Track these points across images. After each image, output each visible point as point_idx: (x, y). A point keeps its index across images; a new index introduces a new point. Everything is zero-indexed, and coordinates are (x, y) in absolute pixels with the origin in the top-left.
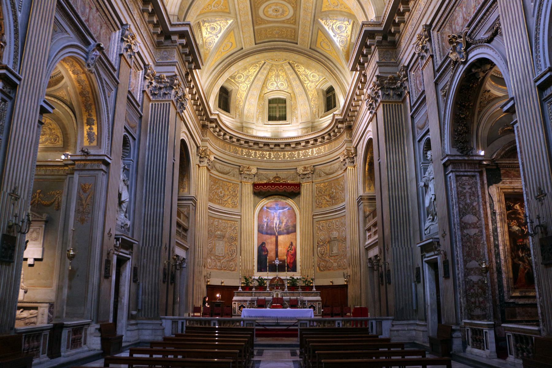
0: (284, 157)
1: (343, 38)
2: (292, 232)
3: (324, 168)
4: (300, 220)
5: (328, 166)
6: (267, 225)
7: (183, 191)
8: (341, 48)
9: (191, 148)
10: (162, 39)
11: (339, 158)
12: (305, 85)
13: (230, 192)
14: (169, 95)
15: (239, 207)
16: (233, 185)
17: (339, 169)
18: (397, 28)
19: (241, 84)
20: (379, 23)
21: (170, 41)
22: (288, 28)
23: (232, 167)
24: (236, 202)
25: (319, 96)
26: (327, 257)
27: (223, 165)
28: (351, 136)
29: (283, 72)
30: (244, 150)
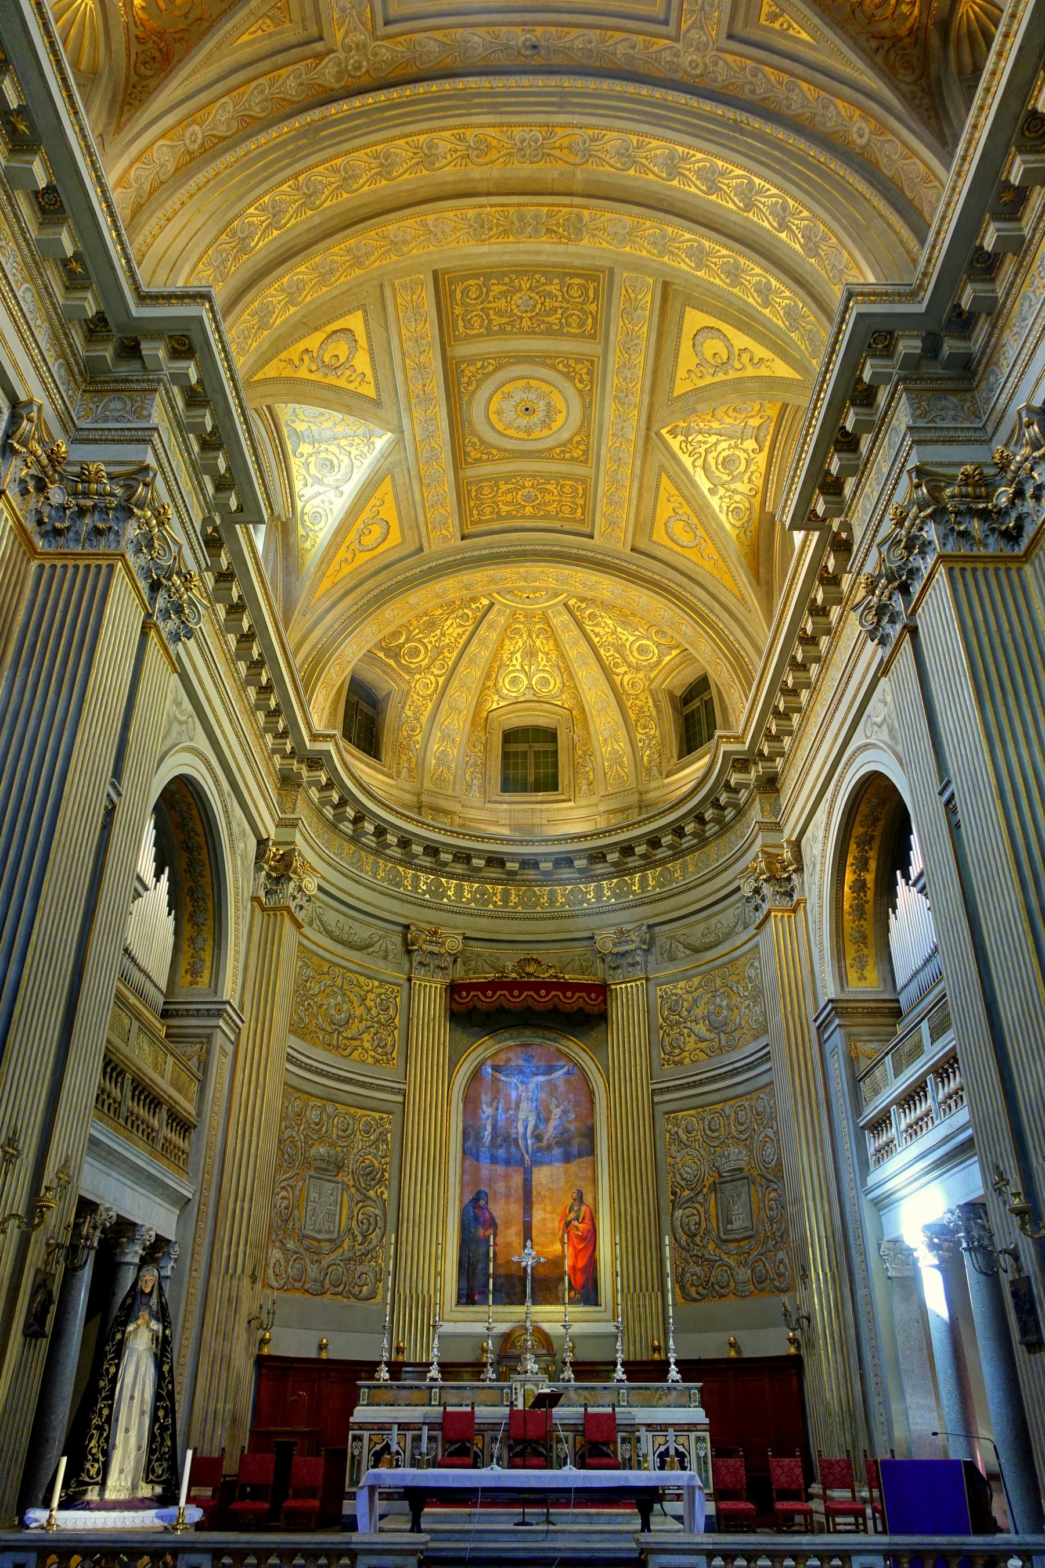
0: (552, 901)
1: (737, 498)
2: (580, 1155)
3: (685, 931)
4: (608, 1108)
5: (698, 922)
6: (494, 1127)
7: (191, 984)
8: (733, 533)
9: (230, 835)
10: (107, 352)
11: (738, 889)
12: (618, 679)
14: (112, 537)
15: (398, 1062)
16: (380, 987)
17: (740, 928)
18: (987, 286)
19: (417, 677)
20: (908, 289)
21: (136, 365)
22: (566, 477)
23: (380, 928)
25: (659, 712)
26: (711, 1247)
27: (351, 917)
28: (776, 810)
29: (547, 639)
30: (423, 877)
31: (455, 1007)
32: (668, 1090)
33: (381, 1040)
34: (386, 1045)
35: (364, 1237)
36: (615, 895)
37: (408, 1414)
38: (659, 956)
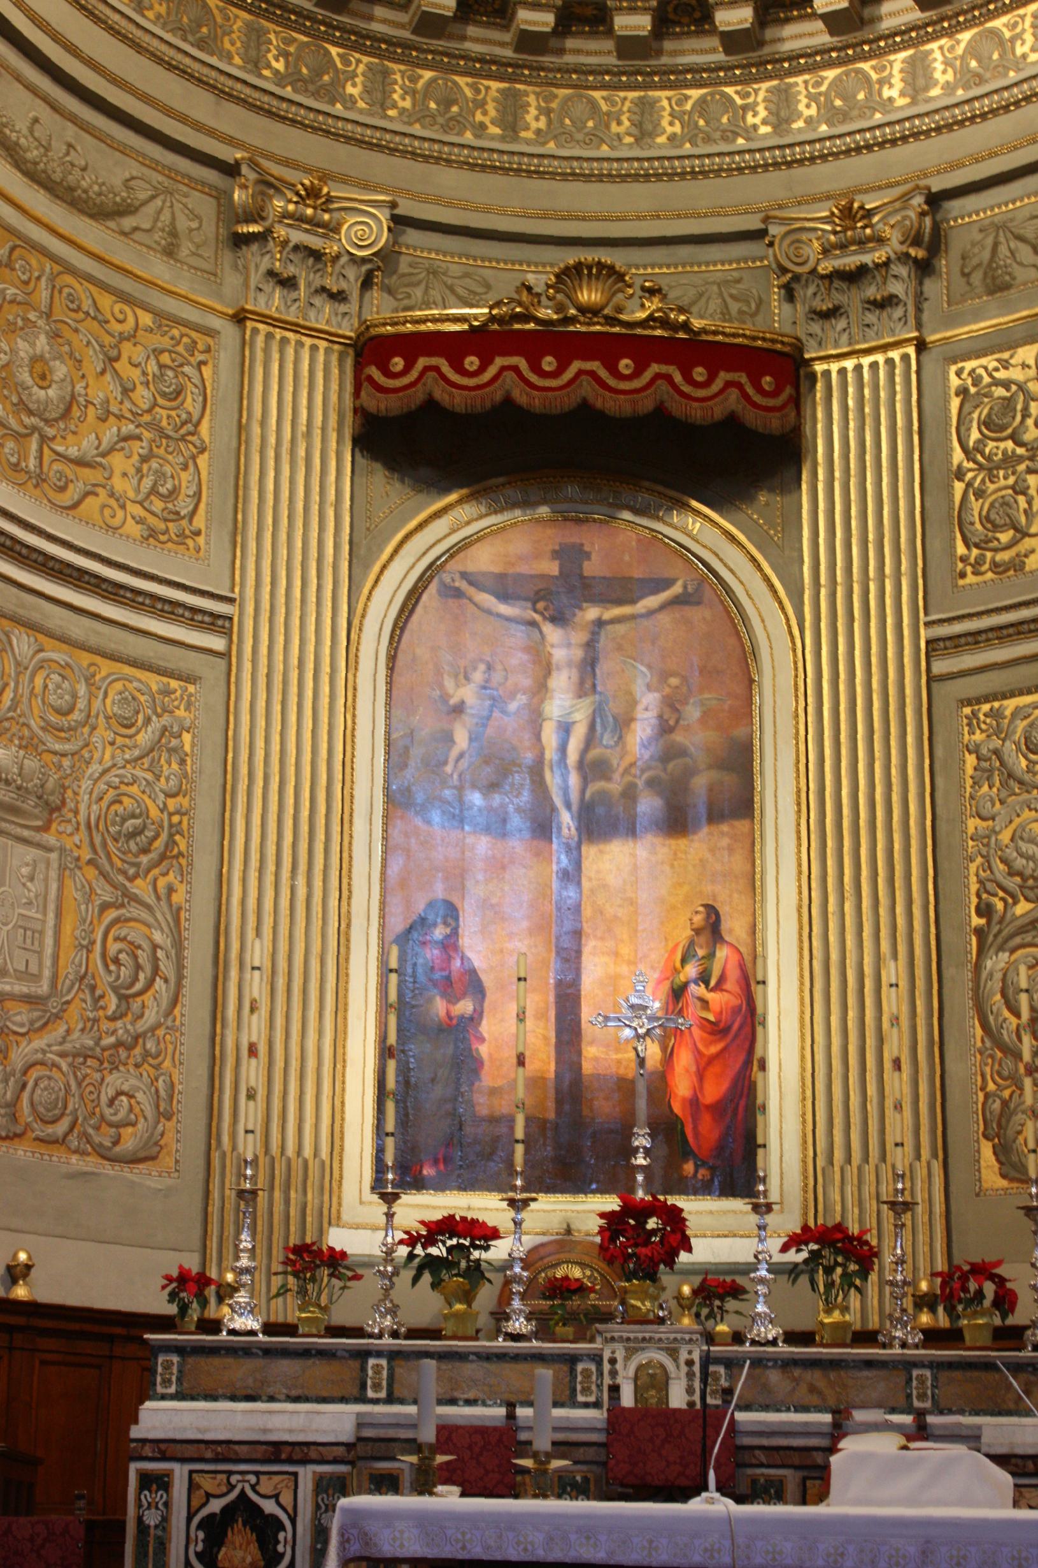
0: (644, 131)
2: (715, 816)
13: (127, 391)
15: (214, 543)
24: (188, 489)
27: (73, 119)
30: (275, 35)
31: (372, 401)
32: (975, 639)
33: (160, 475)
34: (174, 493)
35: (124, 998)
36: (831, 115)
37: (298, 1422)
38: (958, 281)
